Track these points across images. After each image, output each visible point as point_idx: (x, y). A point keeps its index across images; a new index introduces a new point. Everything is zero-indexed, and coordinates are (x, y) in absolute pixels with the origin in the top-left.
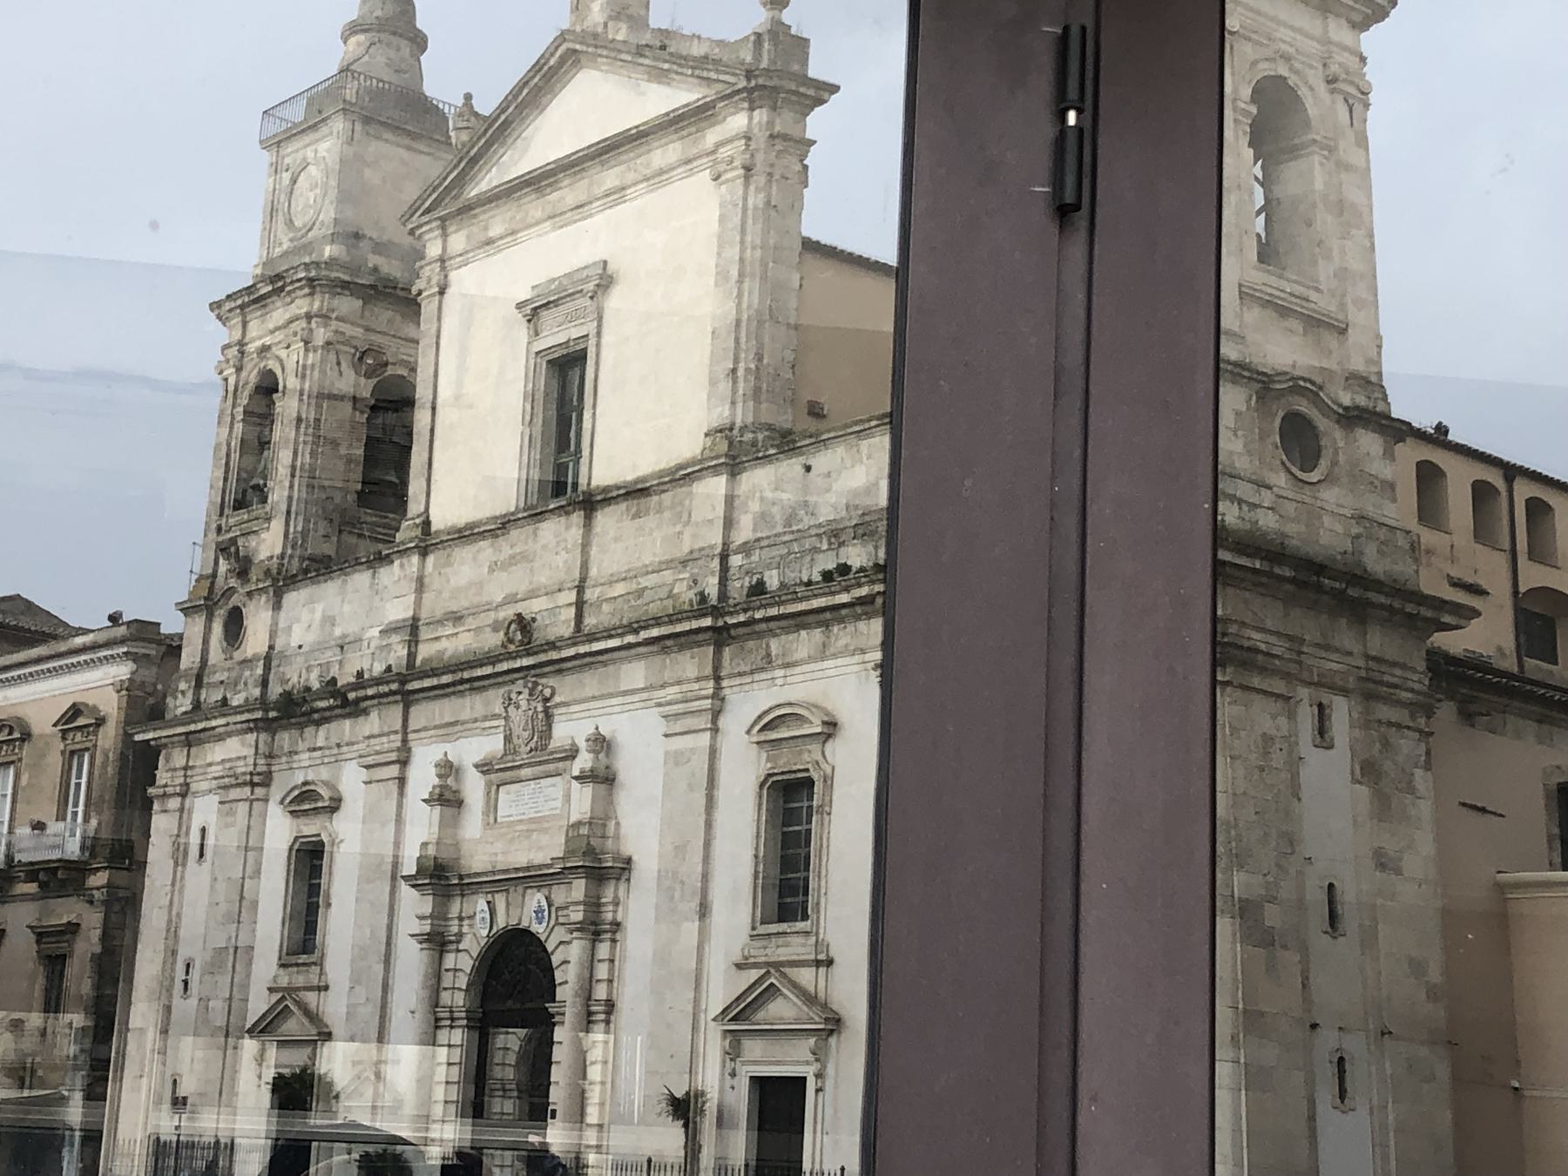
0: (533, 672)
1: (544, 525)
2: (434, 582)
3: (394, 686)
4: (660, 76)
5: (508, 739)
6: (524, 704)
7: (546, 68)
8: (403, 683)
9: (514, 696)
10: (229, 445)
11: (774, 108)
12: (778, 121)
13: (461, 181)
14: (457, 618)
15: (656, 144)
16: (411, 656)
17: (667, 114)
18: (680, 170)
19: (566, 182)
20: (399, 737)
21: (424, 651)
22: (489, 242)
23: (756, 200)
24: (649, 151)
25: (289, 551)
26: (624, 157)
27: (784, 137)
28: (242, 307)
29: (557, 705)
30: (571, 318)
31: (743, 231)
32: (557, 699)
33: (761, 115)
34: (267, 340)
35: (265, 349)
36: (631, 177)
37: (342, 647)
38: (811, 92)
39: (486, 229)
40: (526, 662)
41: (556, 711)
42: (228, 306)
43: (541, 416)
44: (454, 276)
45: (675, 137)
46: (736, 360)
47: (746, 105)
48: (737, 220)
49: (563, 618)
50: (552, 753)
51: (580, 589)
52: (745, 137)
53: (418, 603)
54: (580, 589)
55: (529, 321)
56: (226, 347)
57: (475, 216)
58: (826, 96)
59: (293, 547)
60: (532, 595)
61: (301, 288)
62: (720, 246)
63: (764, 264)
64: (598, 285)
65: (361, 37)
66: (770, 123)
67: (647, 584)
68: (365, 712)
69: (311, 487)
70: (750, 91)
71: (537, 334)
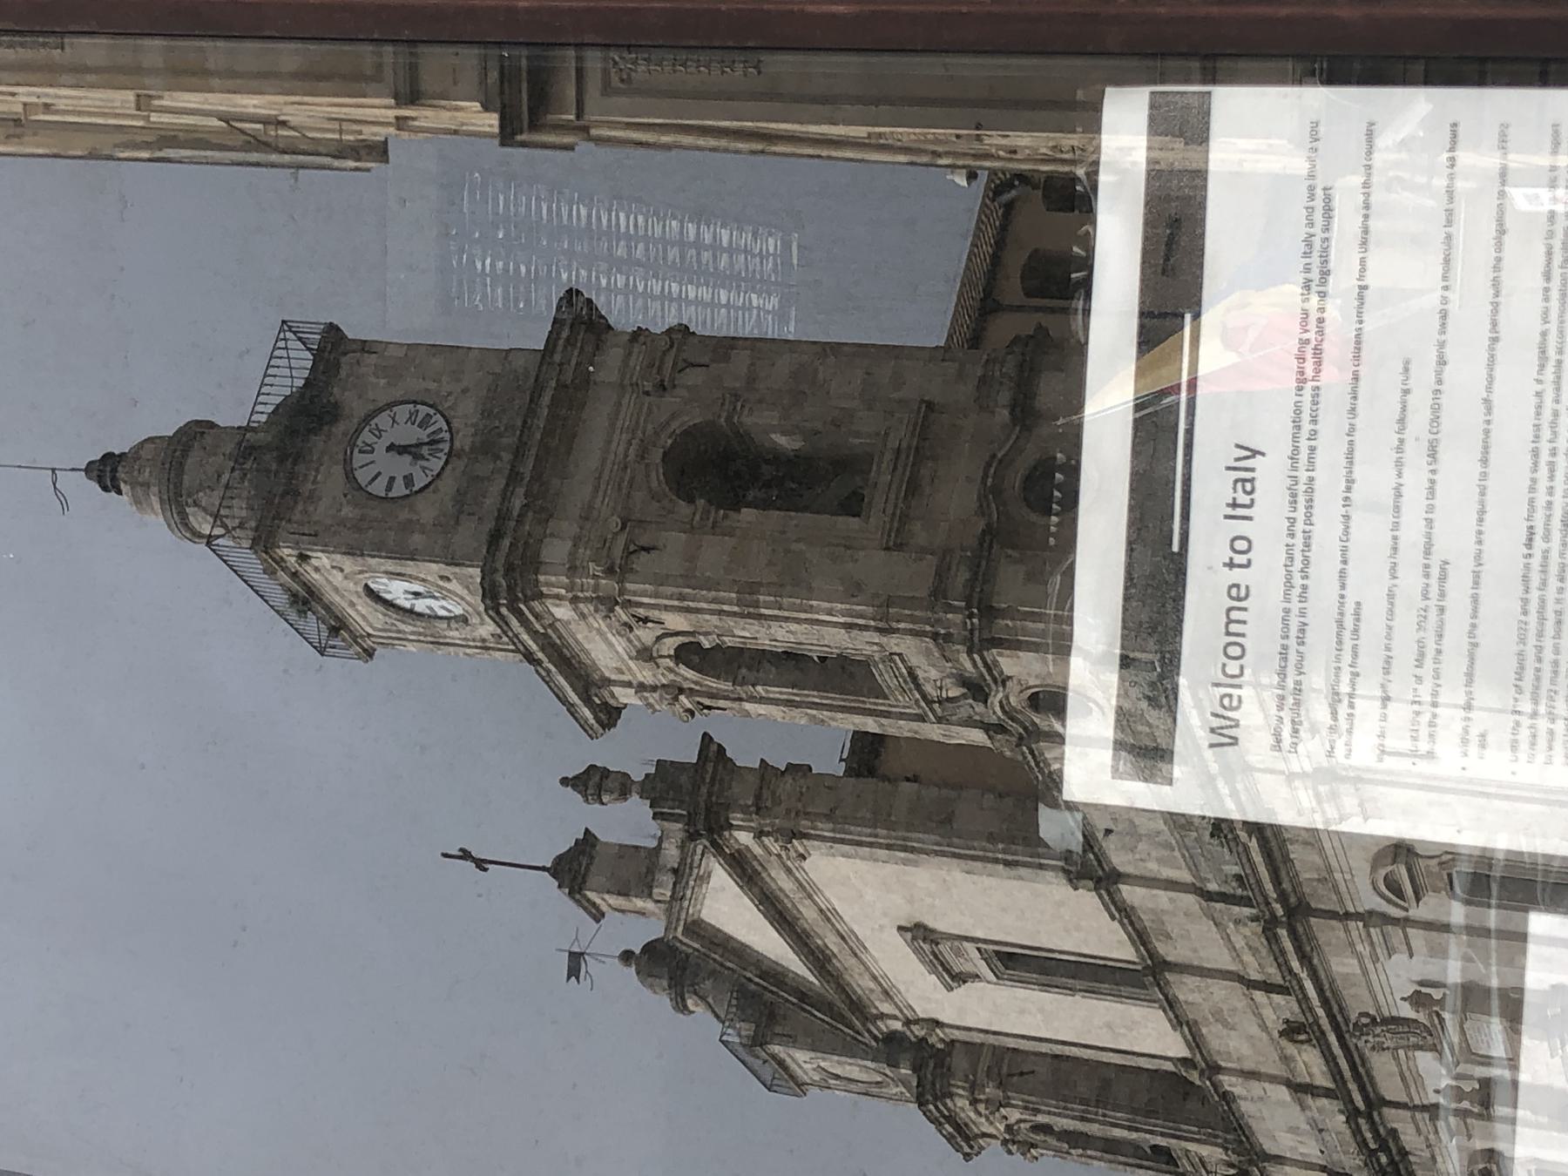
0: (1344, 1028)
1: (1181, 997)
2: (1248, 1065)
3: (1362, 1121)
4: (705, 878)
5: (1421, 1048)
6: (1377, 1039)
7: (703, 950)
8: (1357, 1109)
9: (1369, 1045)
10: (1111, 1162)
11: (728, 807)
12: (741, 802)
13: (828, 1008)
14: (1286, 1059)
15: (773, 886)
16: (1327, 1093)
17: (741, 887)
18: (797, 874)
19: (819, 942)
20: (1418, 1115)
21: (1323, 1080)
22: (886, 993)
23: (824, 828)
24: (781, 889)
25: (1220, 1141)
26: (789, 905)
27: (758, 797)
28: (967, 1139)
29: (1378, 1009)
30: (958, 953)
31: (860, 844)
32: (1372, 1012)
33: (736, 819)
34: (1002, 1128)
35: (1009, 1128)
36: (808, 902)
37: (1321, 1131)
38: (710, 767)
39: (872, 991)
40: (1332, 1038)
41: (1387, 1014)
42: (967, 1149)
43: (1064, 980)
44: (921, 1015)
45: (764, 875)
46: (996, 861)
47: (726, 833)
48: (847, 848)
49: (1283, 1003)
50: (1433, 1025)
51: (1252, 985)
52: (759, 838)
53: (1273, 1079)
54: (1252, 985)
55: (965, 982)
56: (1010, 1152)
57: (859, 998)
58: (714, 748)
59: (1216, 1137)
60: (1259, 1016)
61: (945, 1105)
62: (876, 860)
63: (891, 826)
64: (924, 940)
65: (690, 1002)
66: (744, 810)
67: (1243, 943)
68: (1394, 1133)
69: (1149, 1114)
70: (710, 830)
71: (977, 976)
